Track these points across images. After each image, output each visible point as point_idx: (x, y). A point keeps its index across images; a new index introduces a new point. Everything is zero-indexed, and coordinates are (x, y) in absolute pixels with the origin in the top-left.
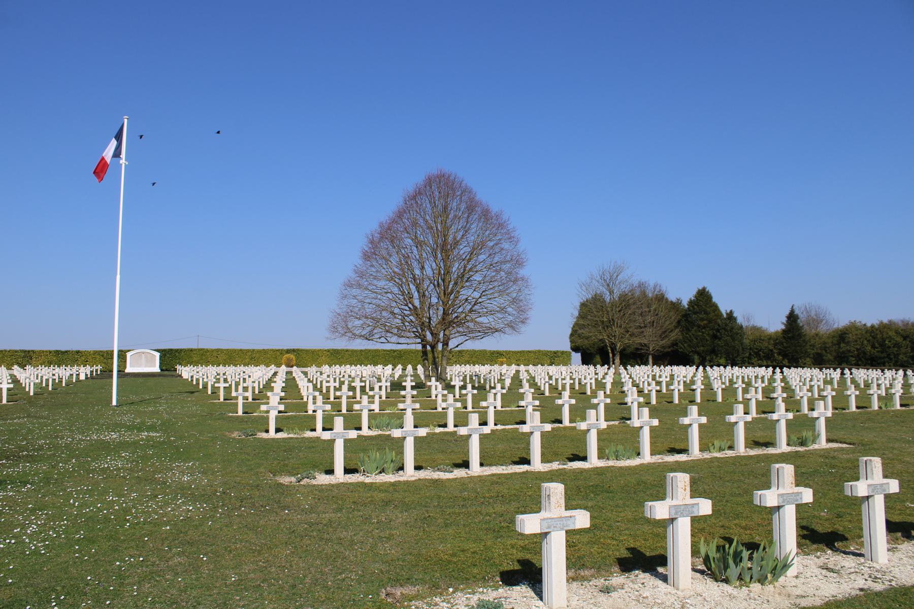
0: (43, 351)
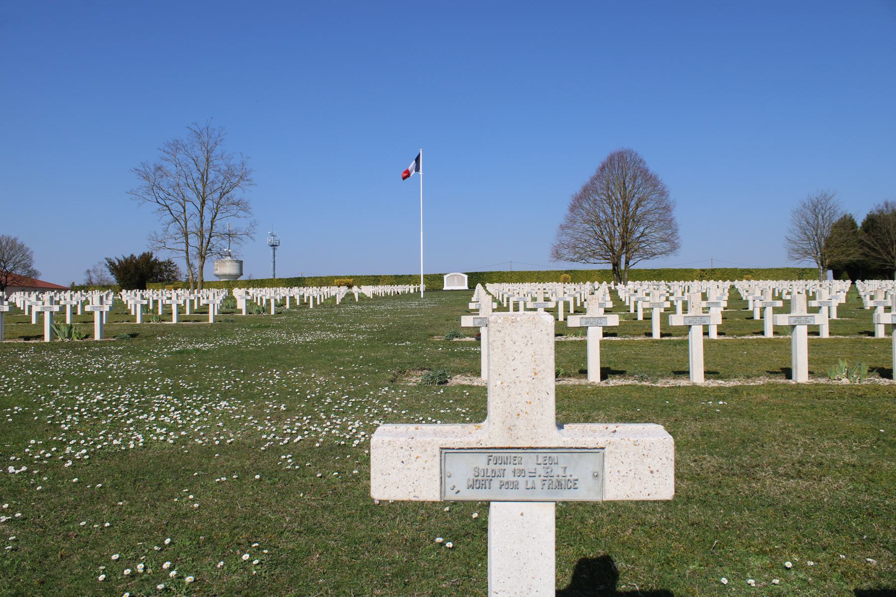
0: (387, 276)
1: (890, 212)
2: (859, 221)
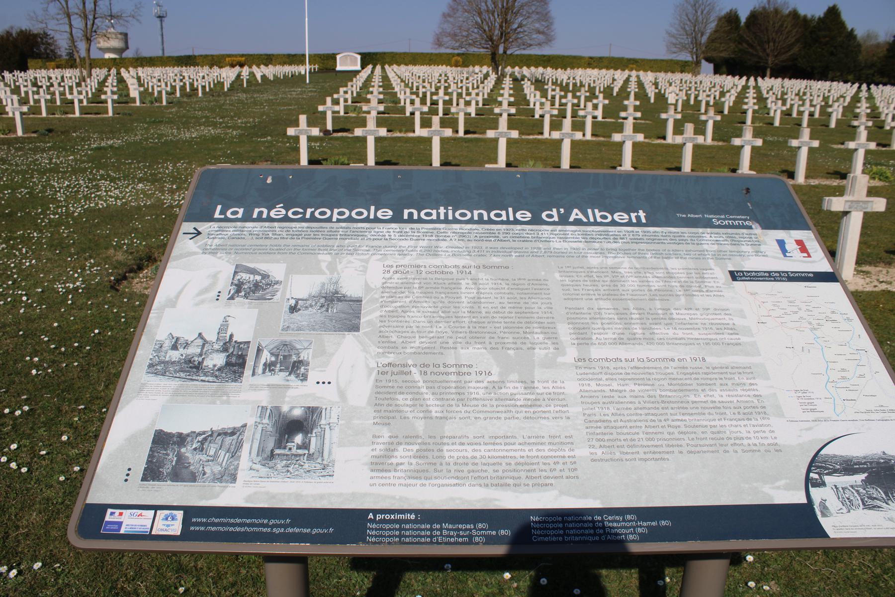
1: (772, 9)
2: (743, 17)
